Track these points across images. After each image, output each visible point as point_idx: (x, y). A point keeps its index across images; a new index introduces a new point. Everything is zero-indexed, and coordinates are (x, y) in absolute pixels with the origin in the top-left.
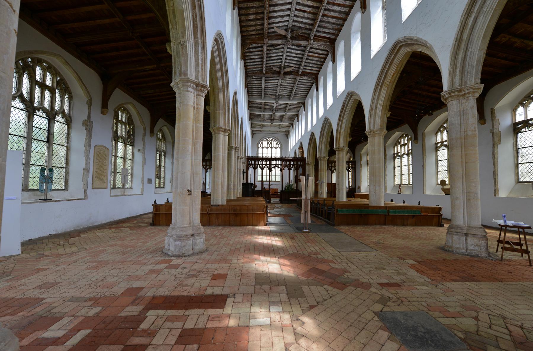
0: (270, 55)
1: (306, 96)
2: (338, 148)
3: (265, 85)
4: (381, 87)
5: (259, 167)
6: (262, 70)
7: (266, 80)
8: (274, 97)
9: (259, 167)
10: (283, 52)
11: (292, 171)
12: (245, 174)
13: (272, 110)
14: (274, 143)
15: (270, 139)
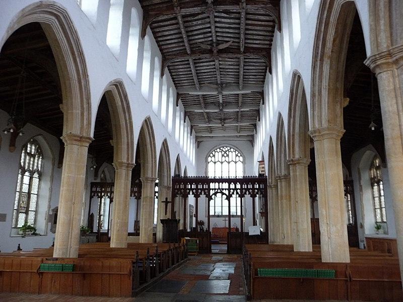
0: (191, 29)
1: (263, 82)
2: (292, 160)
3: (196, 70)
4: (322, 60)
6: (186, 49)
7: (195, 63)
8: (216, 86)
10: (209, 22)
11: (257, 199)
12: (169, 205)
13: (216, 104)
14: (232, 155)
15: (226, 149)
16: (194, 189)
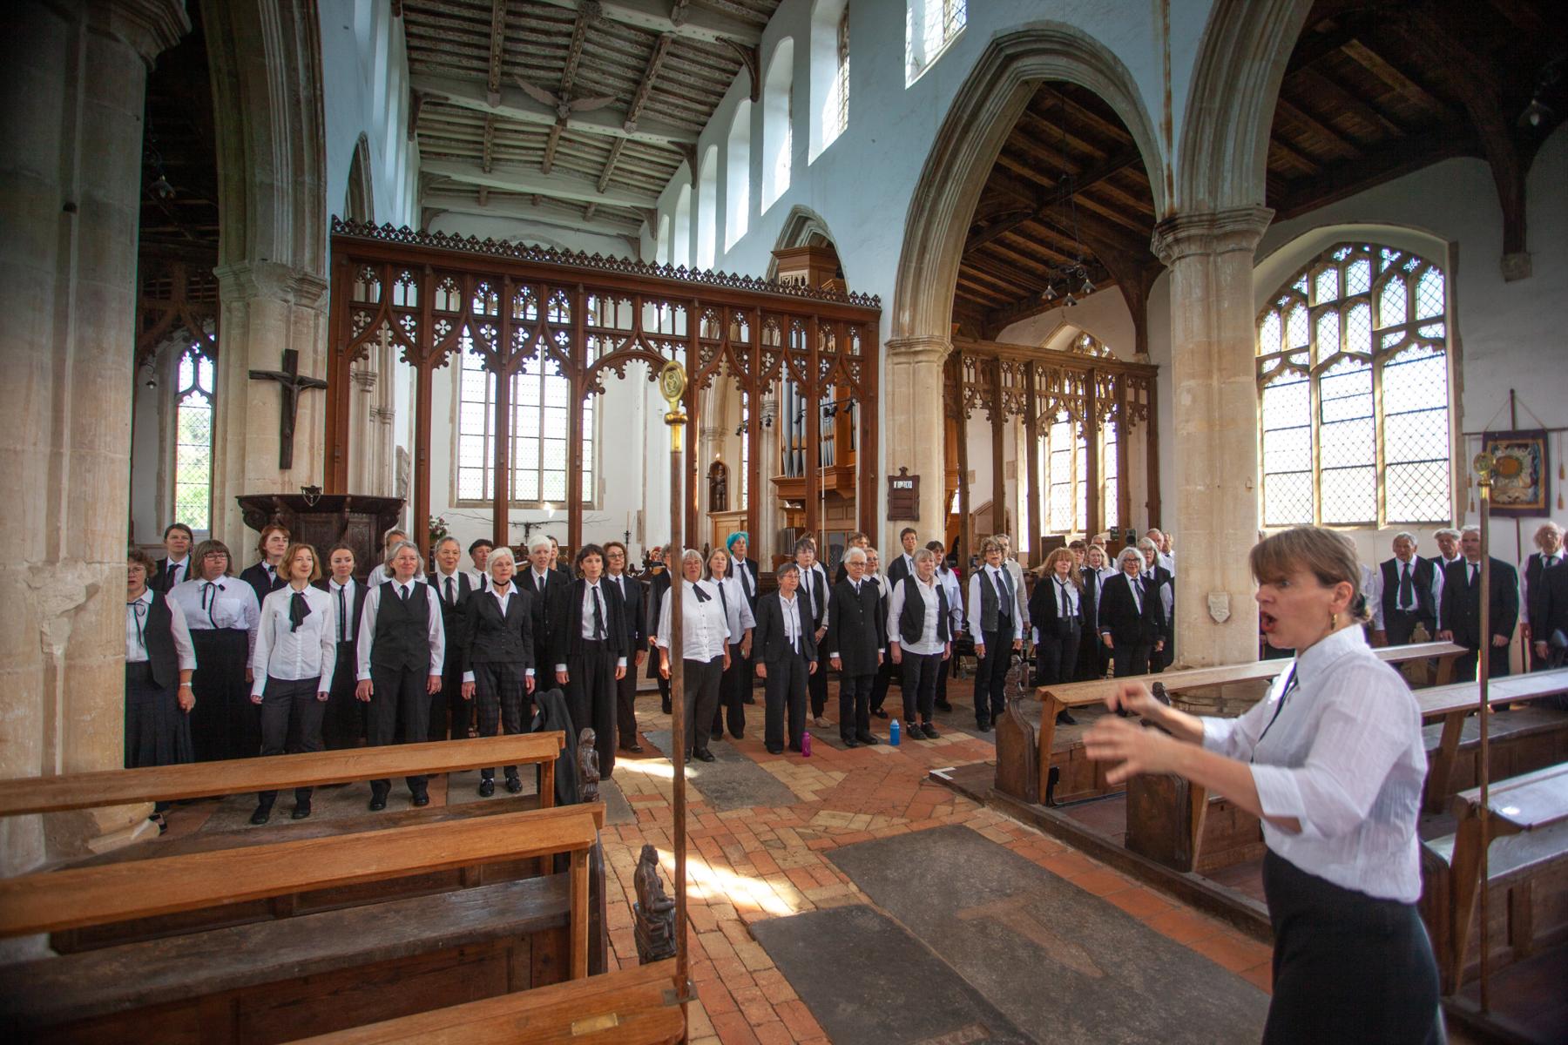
5: (467, 343)
9: (467, 343)
12: (312, 408)
16: (484, 320)
